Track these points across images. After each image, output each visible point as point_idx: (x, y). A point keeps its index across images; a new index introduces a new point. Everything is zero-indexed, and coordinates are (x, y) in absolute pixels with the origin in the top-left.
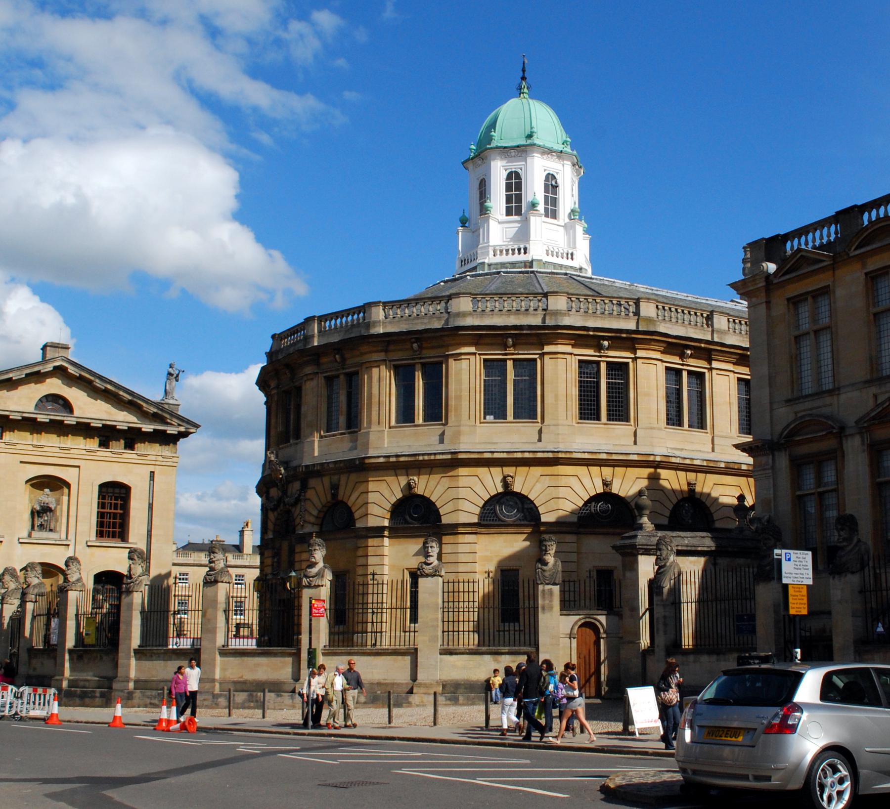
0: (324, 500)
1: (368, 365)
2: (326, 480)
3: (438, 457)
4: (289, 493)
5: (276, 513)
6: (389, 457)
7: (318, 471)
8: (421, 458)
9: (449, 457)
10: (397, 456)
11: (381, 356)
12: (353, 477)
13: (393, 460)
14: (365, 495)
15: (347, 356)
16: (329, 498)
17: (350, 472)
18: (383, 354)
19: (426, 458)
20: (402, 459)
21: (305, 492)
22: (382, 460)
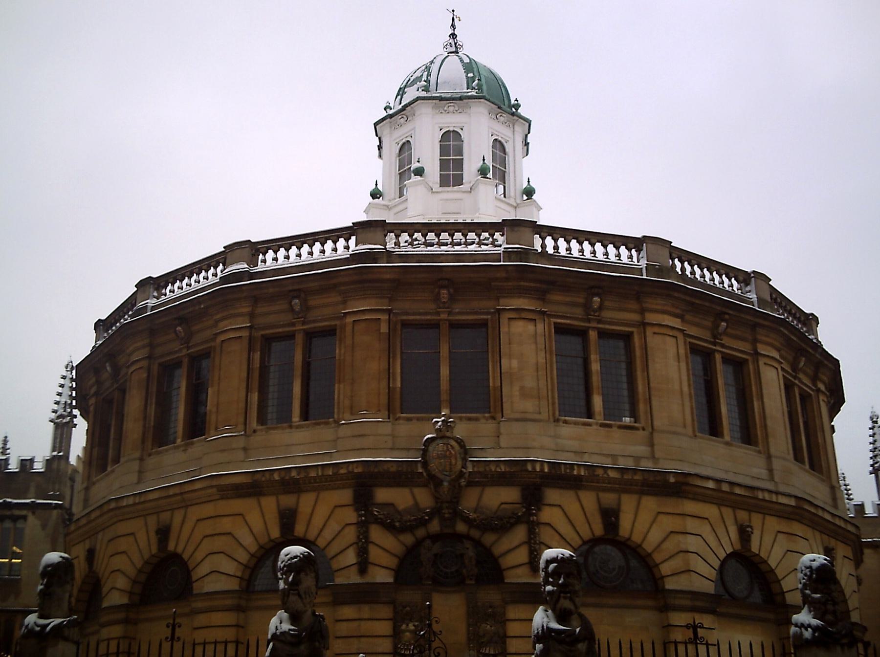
0: (587, 535)
1: (656, 330)
2: (589, 499)
3: (783, 500)
4: (469, 501)
5: (408, 539)
6: (718, 481)
7: (579, 478)
8: (760, 495)
9: (792, 502)
10: (732, 484)
11: (676, 323)
12: (650, 503)
13: (725, 487)
14: (681, 538)
15: (607, 303)
16: (599, 530)
17: (642, 493)
18: (679, 320)
19: (767, 496)
20: (738, 491)
21: (539, 509)
22: (711, 485)
